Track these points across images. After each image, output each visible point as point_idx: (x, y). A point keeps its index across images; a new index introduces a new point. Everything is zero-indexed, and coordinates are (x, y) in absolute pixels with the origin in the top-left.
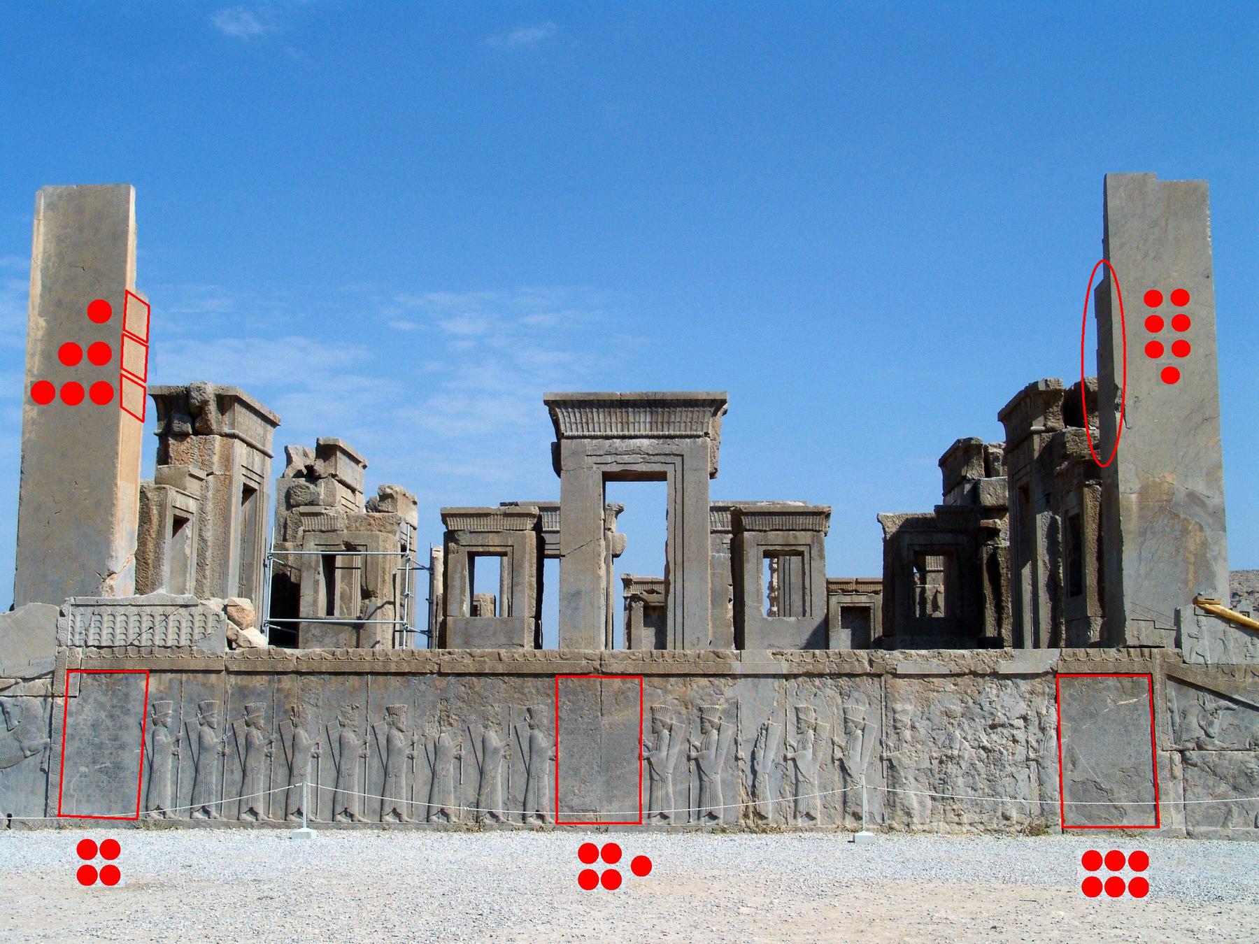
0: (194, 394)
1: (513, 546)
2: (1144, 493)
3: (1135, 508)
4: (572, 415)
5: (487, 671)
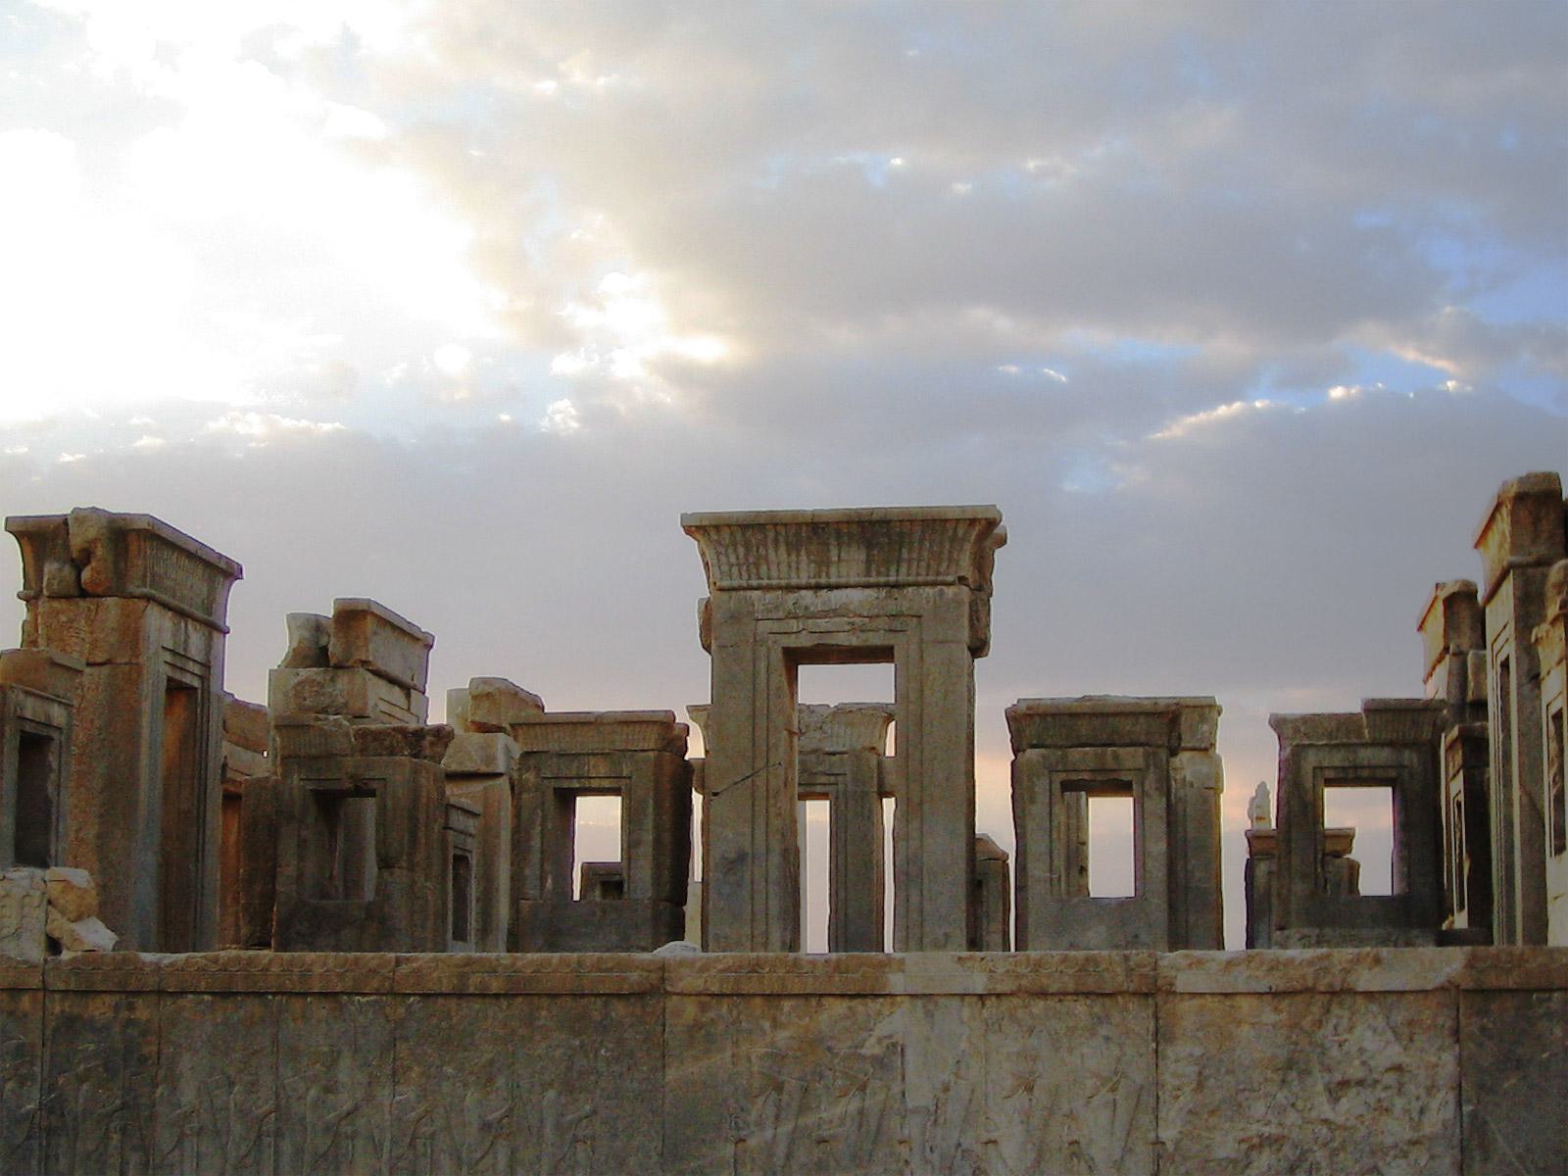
1: (630, 778)
4: (730, 550)
5: (471, 990)
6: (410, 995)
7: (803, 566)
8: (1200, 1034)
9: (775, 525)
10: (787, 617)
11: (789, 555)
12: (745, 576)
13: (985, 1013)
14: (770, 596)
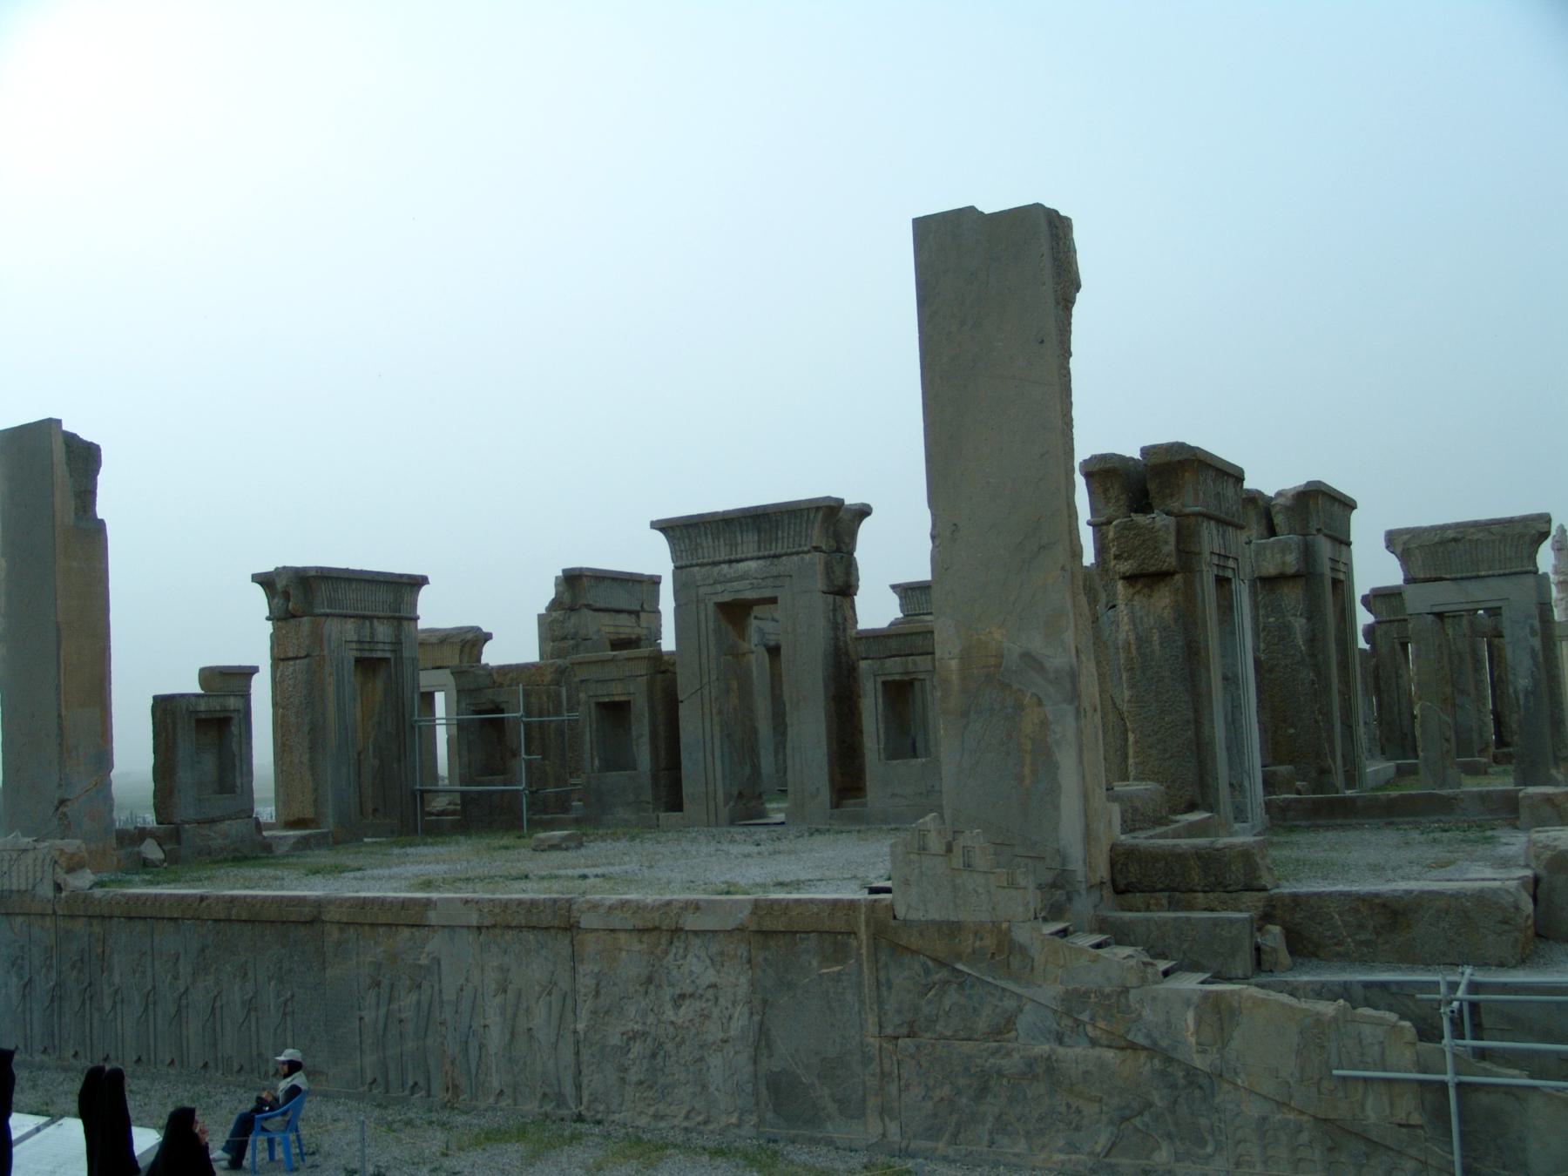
0: (277, 581)
1: (634, 694)
2: (965, 657)
3: (955, 678)
4: (681, 542)
5: (233, 918)
6: (207, 920)
7: (722, 549)
8: (598, 957)
9: (703, 523)
10: (714, 583)
11: (714, 542)
12: (690, 558)
13: (481, 937)
14: (704, 570)
